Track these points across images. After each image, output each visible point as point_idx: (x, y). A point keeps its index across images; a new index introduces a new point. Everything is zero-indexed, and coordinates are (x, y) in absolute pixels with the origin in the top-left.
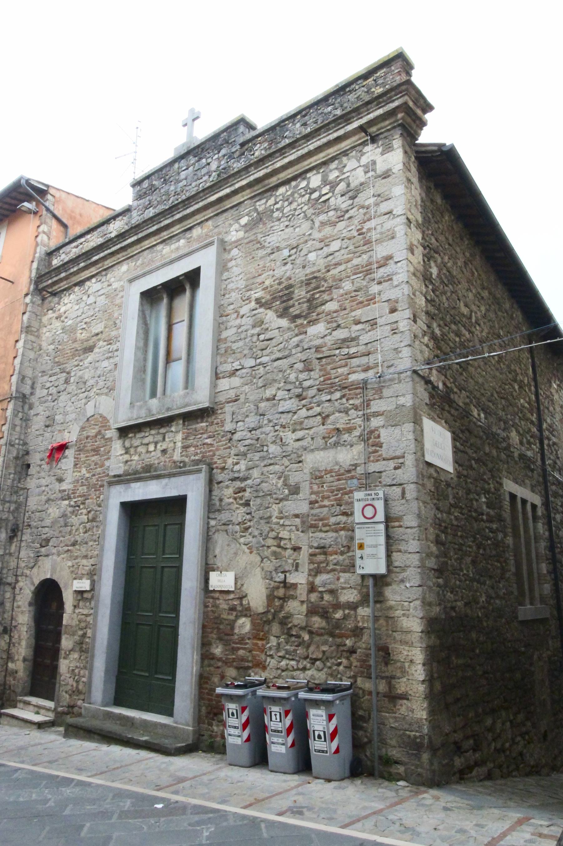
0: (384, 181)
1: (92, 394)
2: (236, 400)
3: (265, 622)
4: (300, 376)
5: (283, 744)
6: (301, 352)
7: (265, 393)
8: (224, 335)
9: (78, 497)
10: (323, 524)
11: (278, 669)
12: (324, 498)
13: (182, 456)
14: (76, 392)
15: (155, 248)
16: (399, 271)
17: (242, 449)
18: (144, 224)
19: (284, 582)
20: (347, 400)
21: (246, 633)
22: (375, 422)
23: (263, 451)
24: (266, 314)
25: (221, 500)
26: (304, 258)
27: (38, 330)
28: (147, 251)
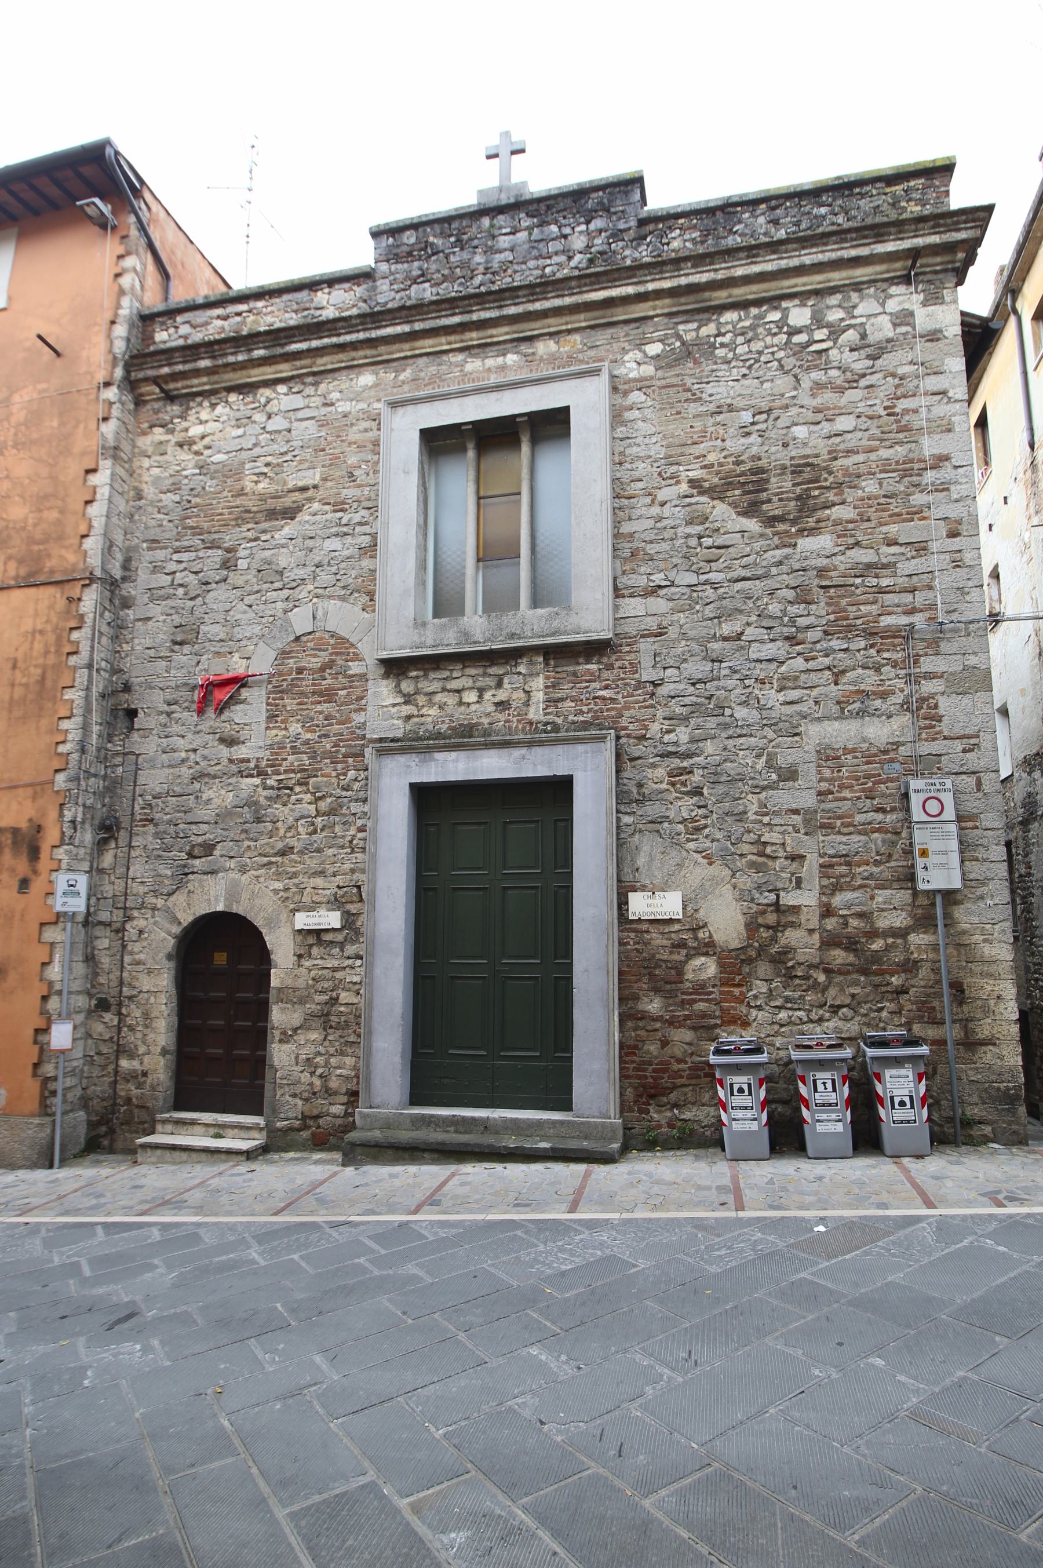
0: (929, 344)
1: (304, 594)
2: (661, 634)
3: (743, 961)
4: (789, 608)
5: (840, 1121)
6: (788, 574)
7: (720, 628)
8: (626, 528)
9: (285, 772)
10: (842, 824)
11: (773, 1023)
12: (842, 787)
13: (546, 714)
14: (256, 588)
15: (445, 358)
16: (960, 480)
17: (679, 710)
18: (432, 307)
19: (777, 903)
20: (878, 652)
21: (709, 978)
22: (928, 687)
23: (723, 715)
24: (714, 507)
25: (640, 785)
26: (784, 431)
27: (130, 460)
28: (425, 359)
